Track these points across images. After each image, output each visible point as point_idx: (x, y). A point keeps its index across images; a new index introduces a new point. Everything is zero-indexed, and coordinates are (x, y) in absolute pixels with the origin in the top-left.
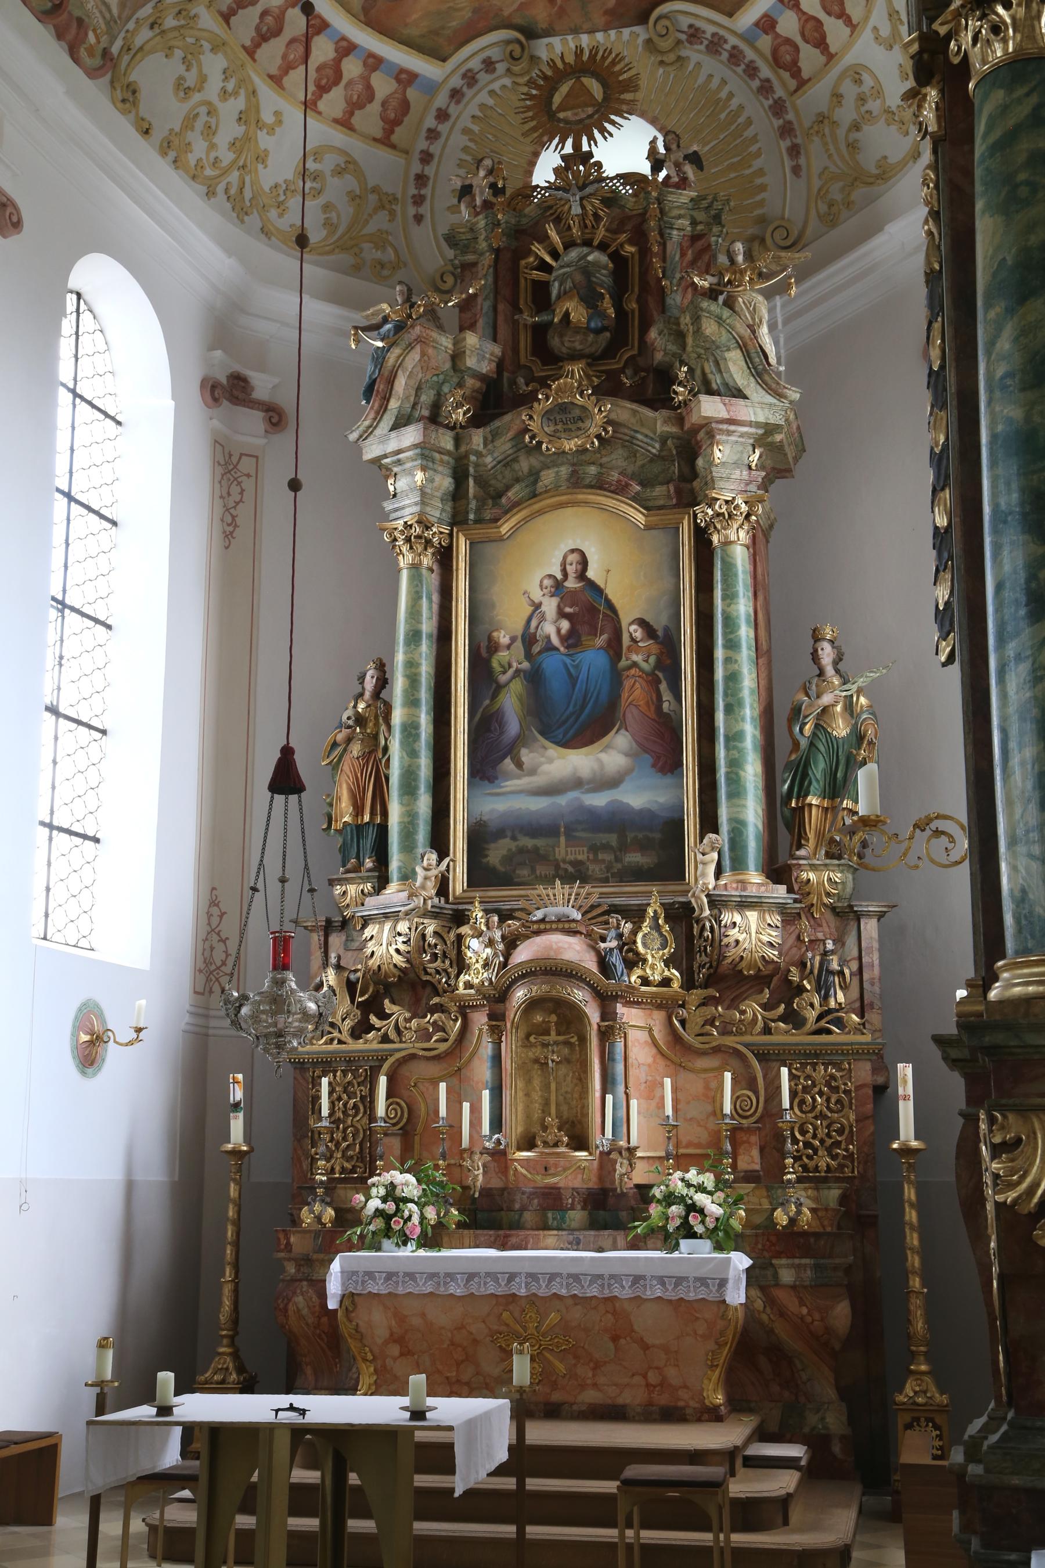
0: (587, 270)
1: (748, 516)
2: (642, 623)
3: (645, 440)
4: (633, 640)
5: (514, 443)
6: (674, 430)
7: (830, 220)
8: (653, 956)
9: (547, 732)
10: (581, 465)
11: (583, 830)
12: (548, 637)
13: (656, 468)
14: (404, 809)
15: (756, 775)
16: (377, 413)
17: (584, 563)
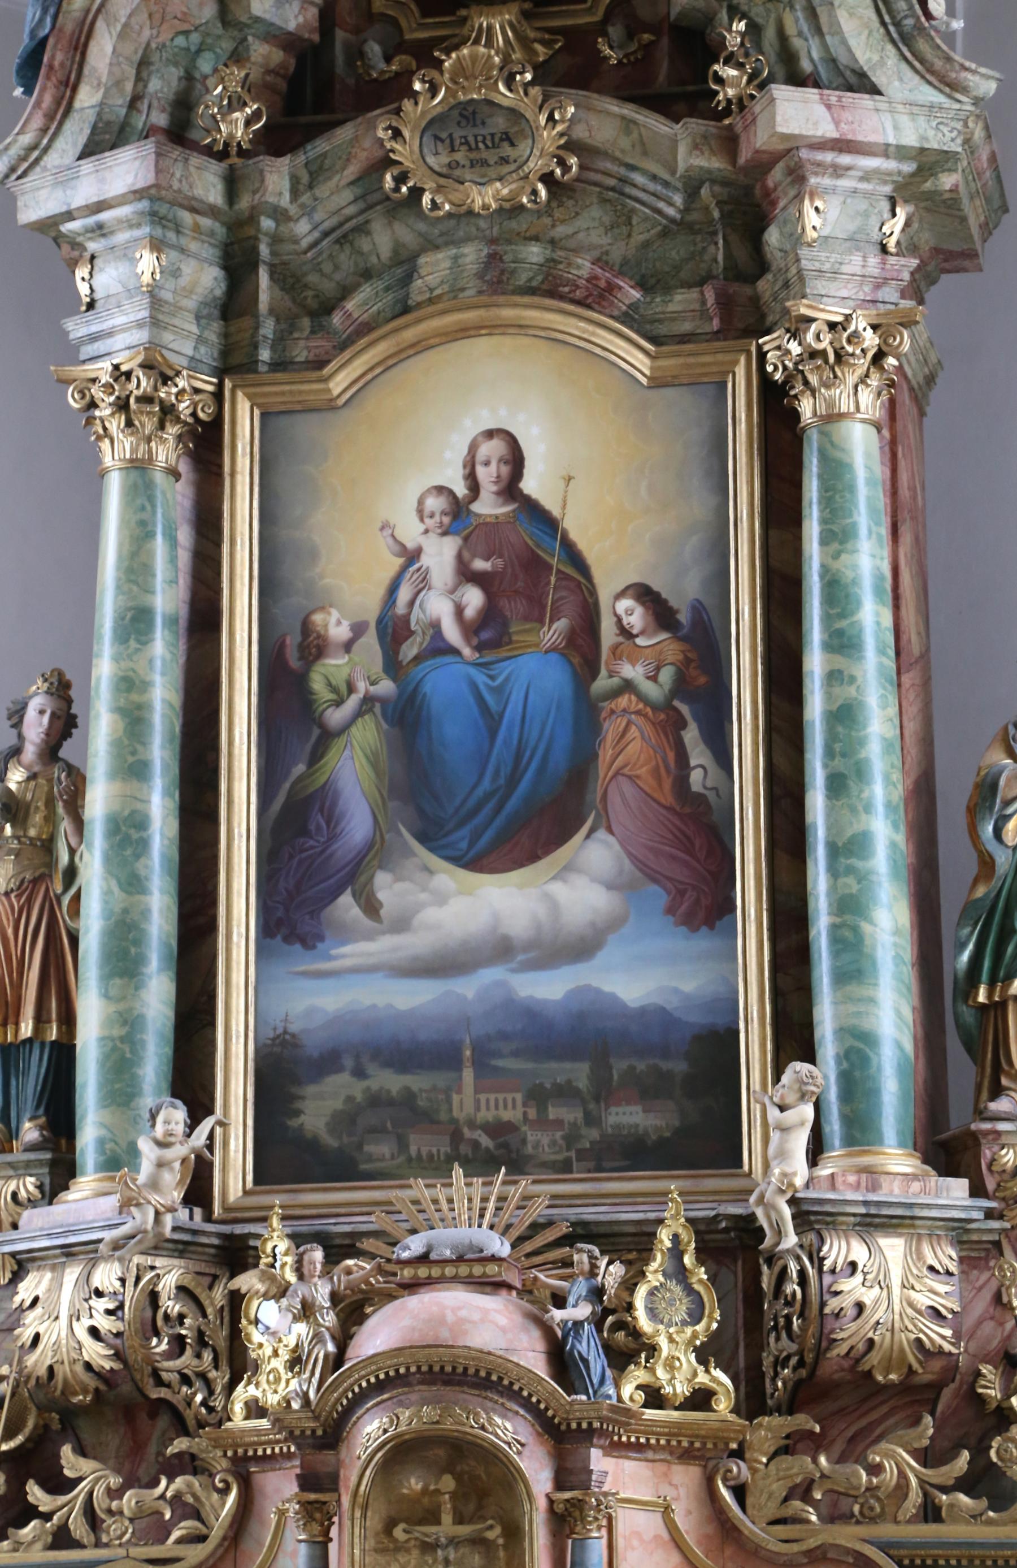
1: (878, 358)
3: (652, 186)
4: (625, 632)
5: (358, 191)
6: (713, 163)
8: (671, 1340)
10: (509, 242)
11: (516, 1054)
12: (436, 626)
13: (676, 251)
14: (112, 1008)
15: (897, 932)
16: (50, 117)
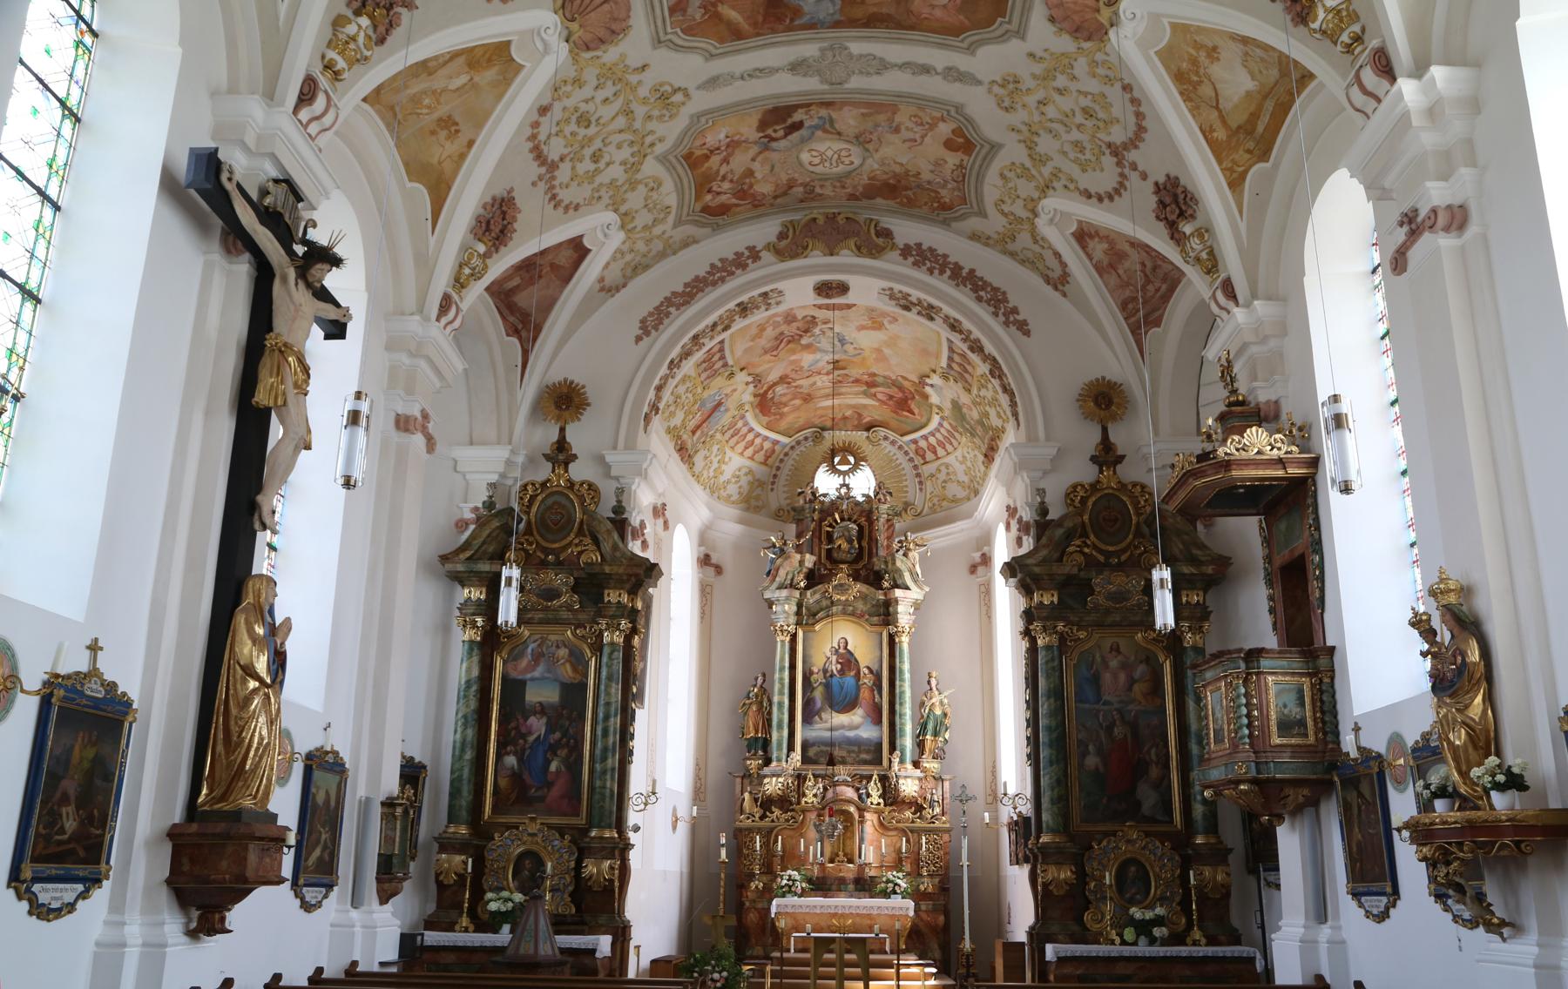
0: (848, 530)
2: (868, 668)
9: (831, 707)
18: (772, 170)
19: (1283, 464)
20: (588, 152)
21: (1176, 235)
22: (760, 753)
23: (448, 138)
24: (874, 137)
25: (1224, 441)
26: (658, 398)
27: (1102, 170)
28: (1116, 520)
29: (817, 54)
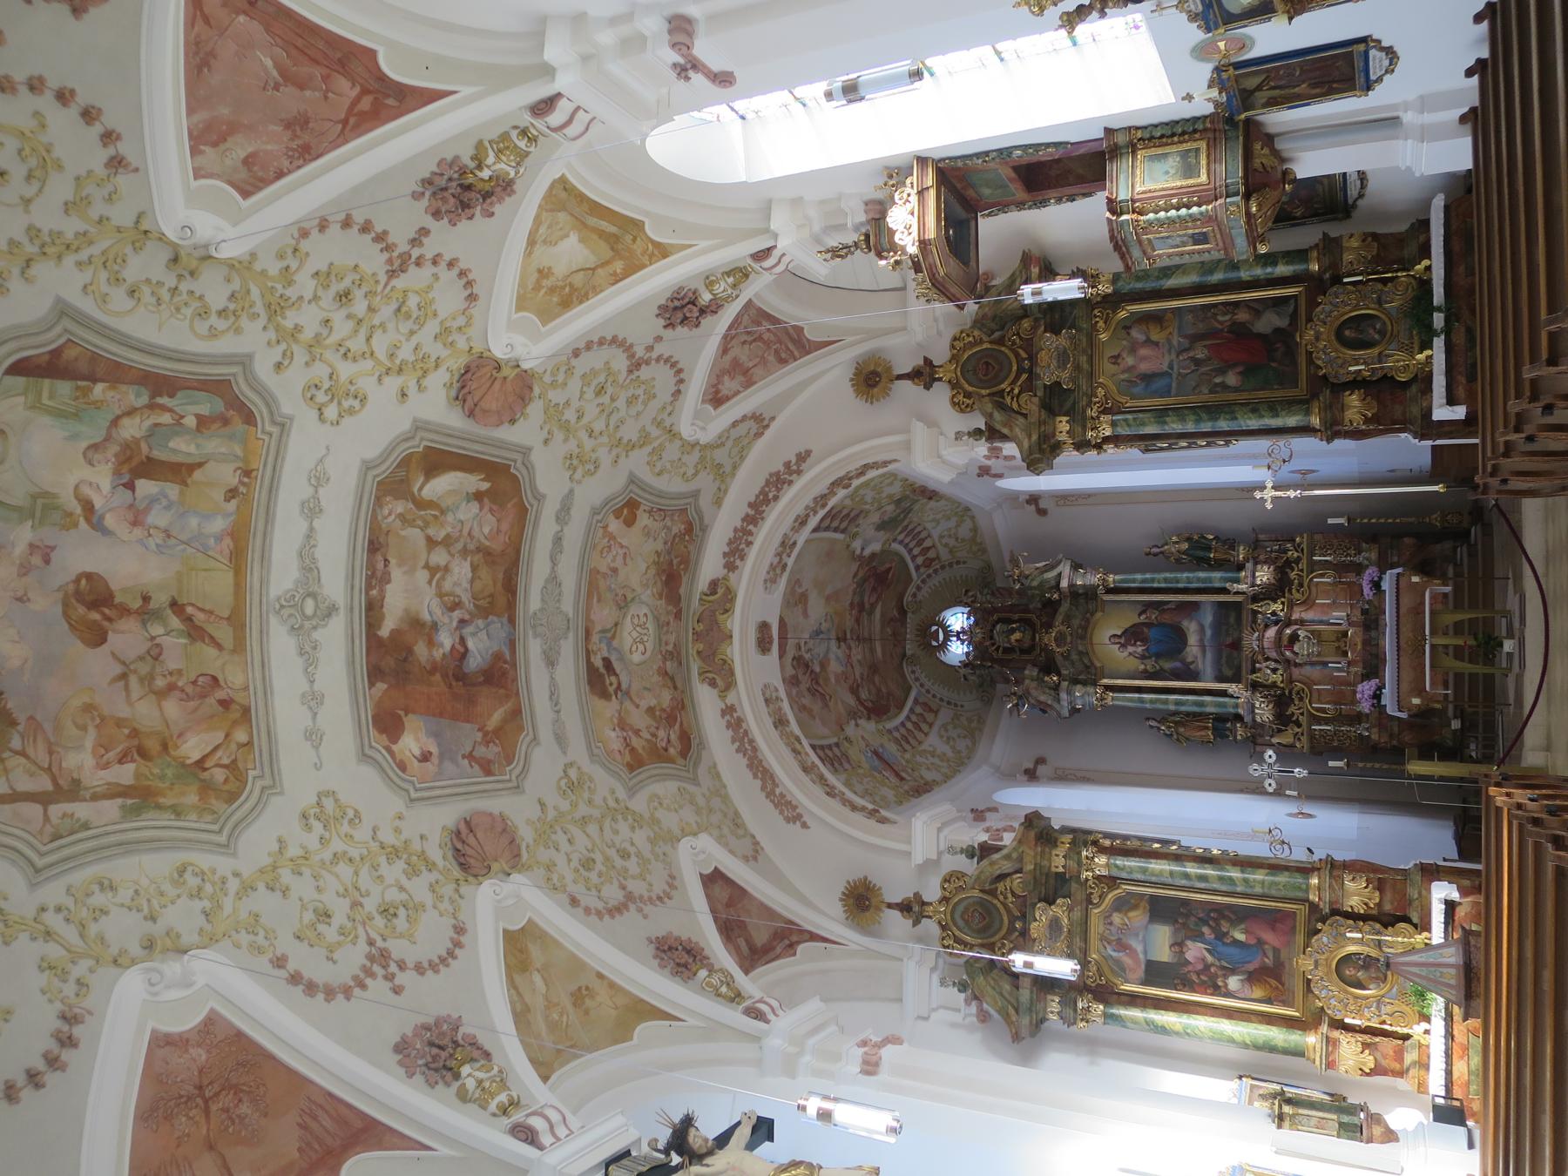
7: (984, 551)
17: (1115, 636)
18: (649, 690)
19: (923, 190)
20: (618, 862)
21: (713, 308)
22: (1229, 725)
23: (592, 997)
24: (621, 592)
25: (903, 249)
26: (863, 809)
27: (654, 379)
28: (987, 364)
29: (538, 641)
